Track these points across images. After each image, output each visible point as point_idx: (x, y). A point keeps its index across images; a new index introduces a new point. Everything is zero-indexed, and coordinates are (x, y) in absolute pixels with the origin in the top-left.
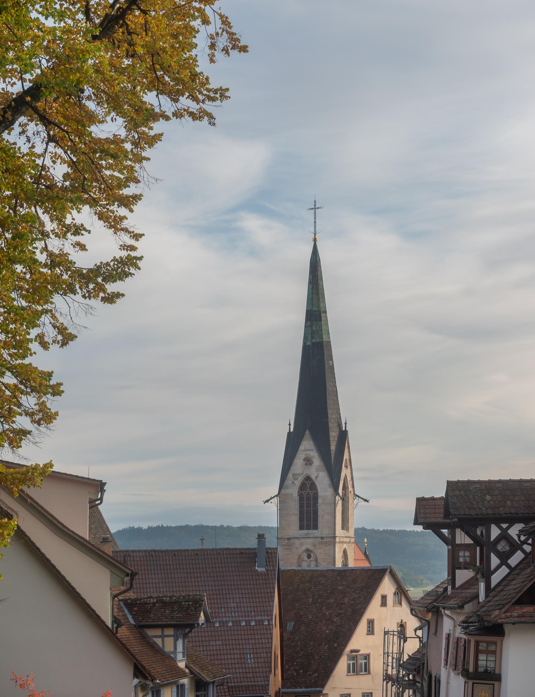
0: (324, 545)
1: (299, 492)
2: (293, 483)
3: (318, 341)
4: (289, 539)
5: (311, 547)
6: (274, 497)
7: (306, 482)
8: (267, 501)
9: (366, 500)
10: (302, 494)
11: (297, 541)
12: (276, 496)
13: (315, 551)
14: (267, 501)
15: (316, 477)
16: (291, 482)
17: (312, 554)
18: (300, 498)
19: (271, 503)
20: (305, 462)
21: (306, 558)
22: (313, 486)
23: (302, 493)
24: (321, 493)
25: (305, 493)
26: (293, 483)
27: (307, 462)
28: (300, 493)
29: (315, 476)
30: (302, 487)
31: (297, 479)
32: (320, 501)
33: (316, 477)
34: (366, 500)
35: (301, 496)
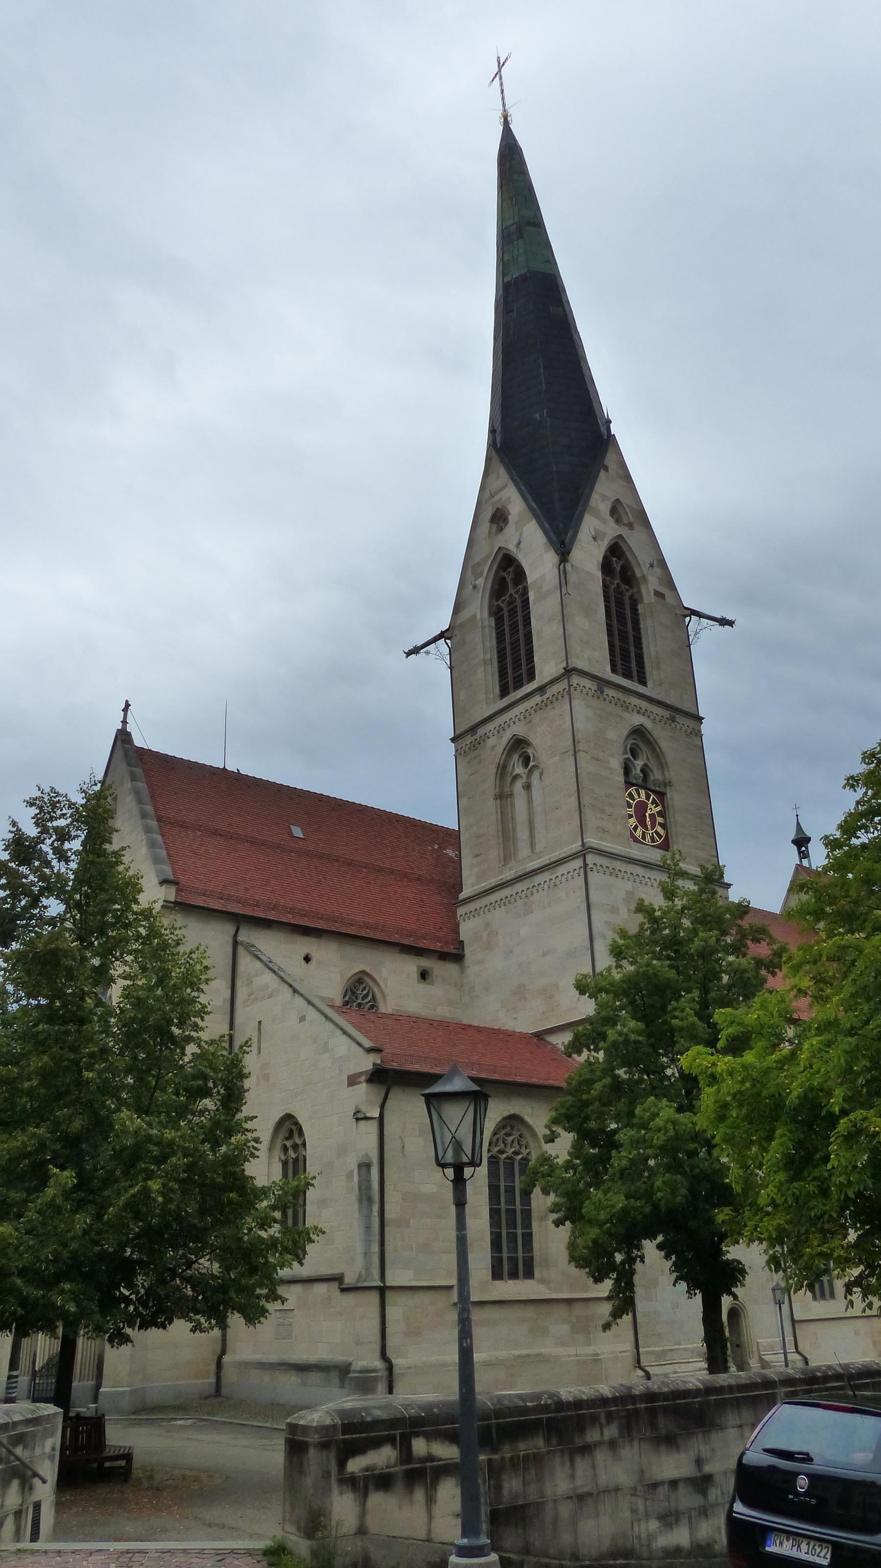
0: (550, 706)
1: (490, 606)
2: (475, 587)
3: (516, 275)
4: (473, 729)
5: (519, 729)
6: (434, 640)
7: (504, 574)
8: (415, 651)
9: (724, 622)
10: (500, 609)
11: (490, 726)
12: (442, 635)
13: (532, 738)
14: (415, 651)
15: (519, 543)
16: (471, 587)
17: (530, 751)
18: (496, 620)
19: (428, 653)
20: (495, 526)
21: (519, 770)
22: (520, 575)
23: (498, 606)
24: (532, 576)
25: (503, 602)
26: (475, 587)
27: (502, 524)
28: (494, 609)
29: (516, 542)
30: (499, 589)
31: (481, 575)
32: (532, 595)
33: (519, 543)
34: (724, 622)
35: (496, 613)
